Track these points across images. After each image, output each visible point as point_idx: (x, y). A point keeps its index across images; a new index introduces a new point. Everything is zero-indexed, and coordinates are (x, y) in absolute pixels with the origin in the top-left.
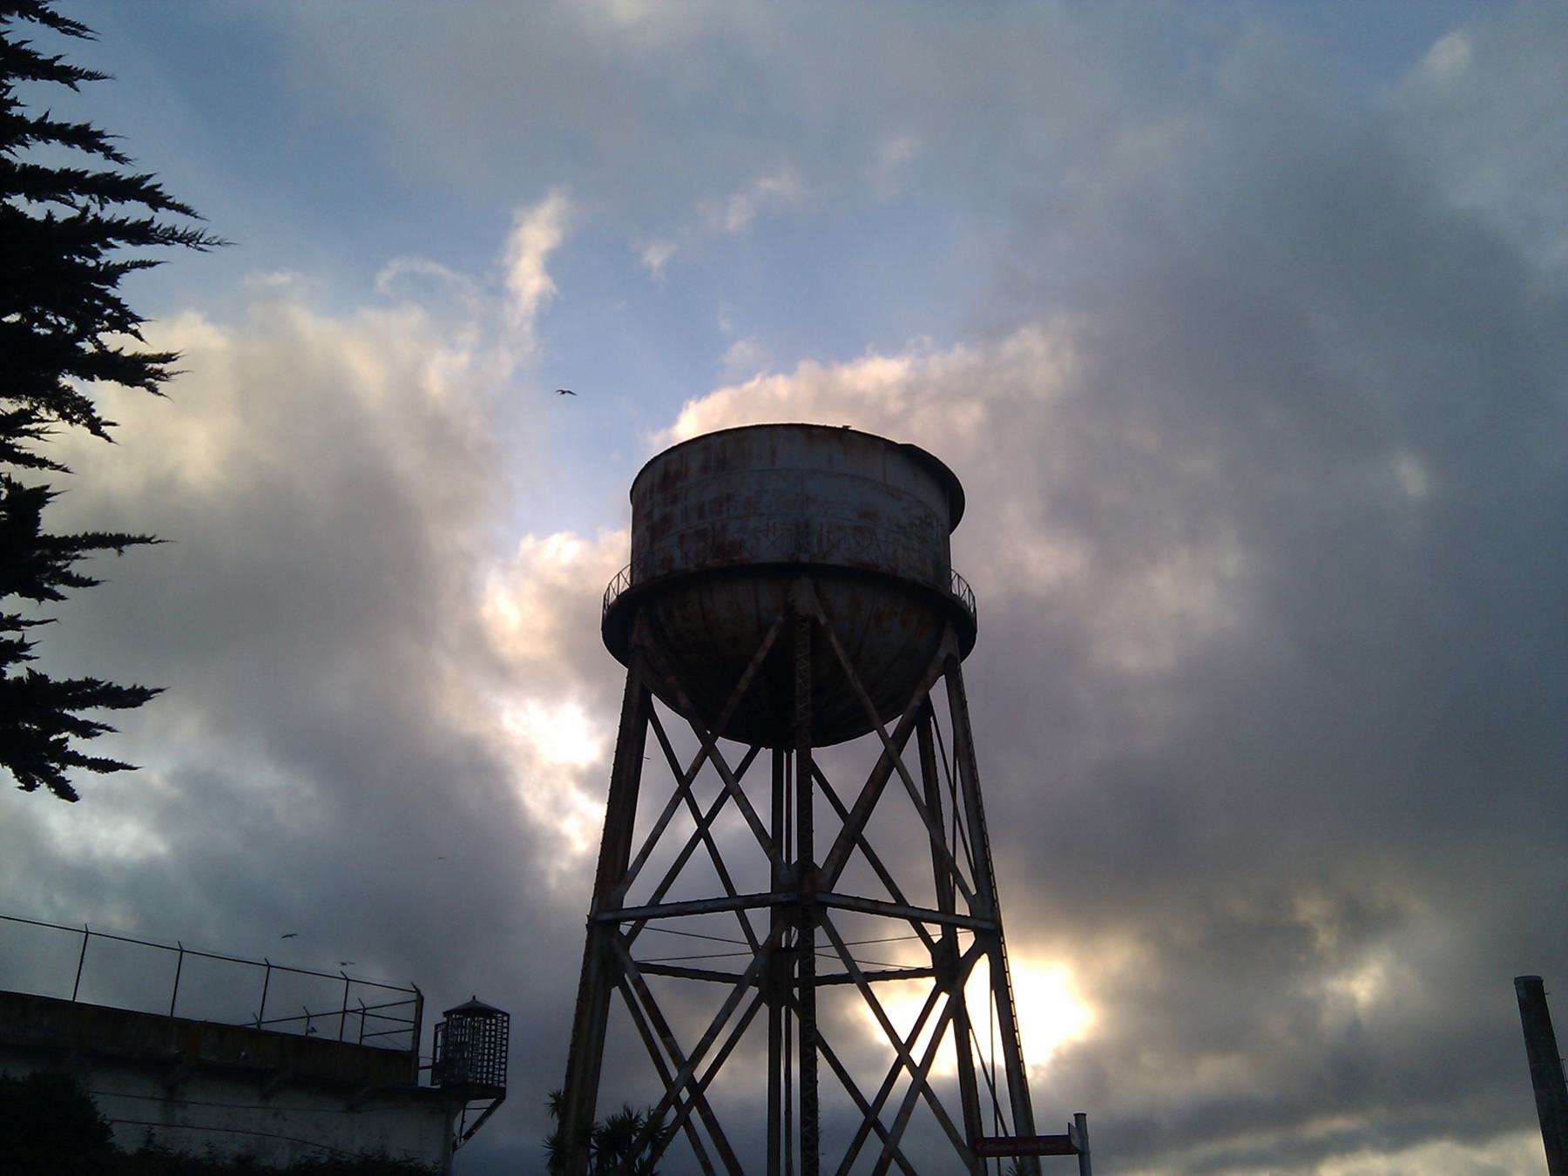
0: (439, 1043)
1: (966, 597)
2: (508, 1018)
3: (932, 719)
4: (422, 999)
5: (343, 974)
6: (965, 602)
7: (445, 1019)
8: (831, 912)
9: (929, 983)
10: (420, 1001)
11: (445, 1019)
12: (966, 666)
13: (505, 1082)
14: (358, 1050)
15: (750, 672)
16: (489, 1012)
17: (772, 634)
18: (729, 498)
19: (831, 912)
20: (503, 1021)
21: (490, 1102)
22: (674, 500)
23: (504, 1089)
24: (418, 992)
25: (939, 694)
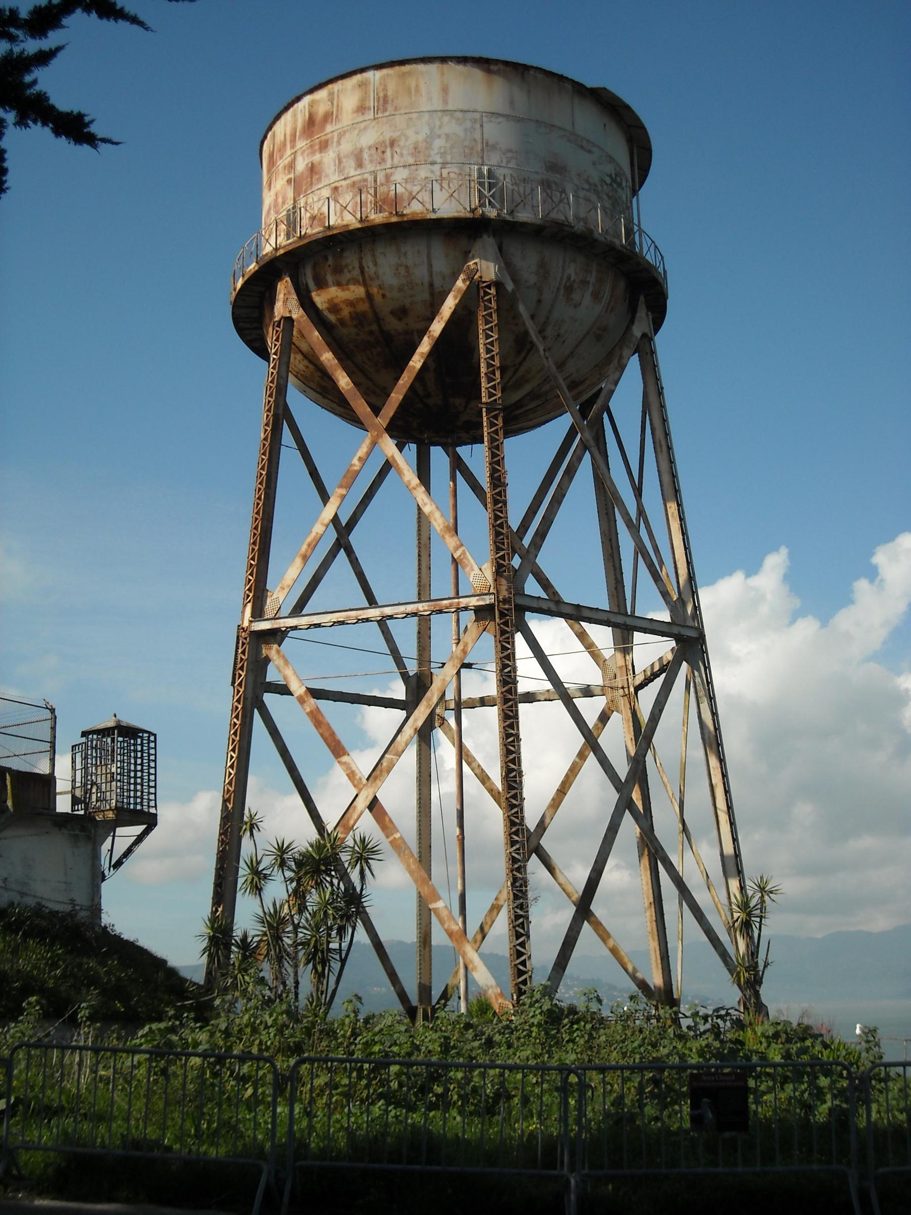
0: (78, 766)
1: (661, 270)
2: (155, 738)
4: (56, 717)
7: (84, 740)
13: (156, 807)
15: (425, 346)
16: (129, 732)
17: (450, 304)
18: (392, 143)
21: (139, 829)
22: (324, 146)
23: (156, 815)
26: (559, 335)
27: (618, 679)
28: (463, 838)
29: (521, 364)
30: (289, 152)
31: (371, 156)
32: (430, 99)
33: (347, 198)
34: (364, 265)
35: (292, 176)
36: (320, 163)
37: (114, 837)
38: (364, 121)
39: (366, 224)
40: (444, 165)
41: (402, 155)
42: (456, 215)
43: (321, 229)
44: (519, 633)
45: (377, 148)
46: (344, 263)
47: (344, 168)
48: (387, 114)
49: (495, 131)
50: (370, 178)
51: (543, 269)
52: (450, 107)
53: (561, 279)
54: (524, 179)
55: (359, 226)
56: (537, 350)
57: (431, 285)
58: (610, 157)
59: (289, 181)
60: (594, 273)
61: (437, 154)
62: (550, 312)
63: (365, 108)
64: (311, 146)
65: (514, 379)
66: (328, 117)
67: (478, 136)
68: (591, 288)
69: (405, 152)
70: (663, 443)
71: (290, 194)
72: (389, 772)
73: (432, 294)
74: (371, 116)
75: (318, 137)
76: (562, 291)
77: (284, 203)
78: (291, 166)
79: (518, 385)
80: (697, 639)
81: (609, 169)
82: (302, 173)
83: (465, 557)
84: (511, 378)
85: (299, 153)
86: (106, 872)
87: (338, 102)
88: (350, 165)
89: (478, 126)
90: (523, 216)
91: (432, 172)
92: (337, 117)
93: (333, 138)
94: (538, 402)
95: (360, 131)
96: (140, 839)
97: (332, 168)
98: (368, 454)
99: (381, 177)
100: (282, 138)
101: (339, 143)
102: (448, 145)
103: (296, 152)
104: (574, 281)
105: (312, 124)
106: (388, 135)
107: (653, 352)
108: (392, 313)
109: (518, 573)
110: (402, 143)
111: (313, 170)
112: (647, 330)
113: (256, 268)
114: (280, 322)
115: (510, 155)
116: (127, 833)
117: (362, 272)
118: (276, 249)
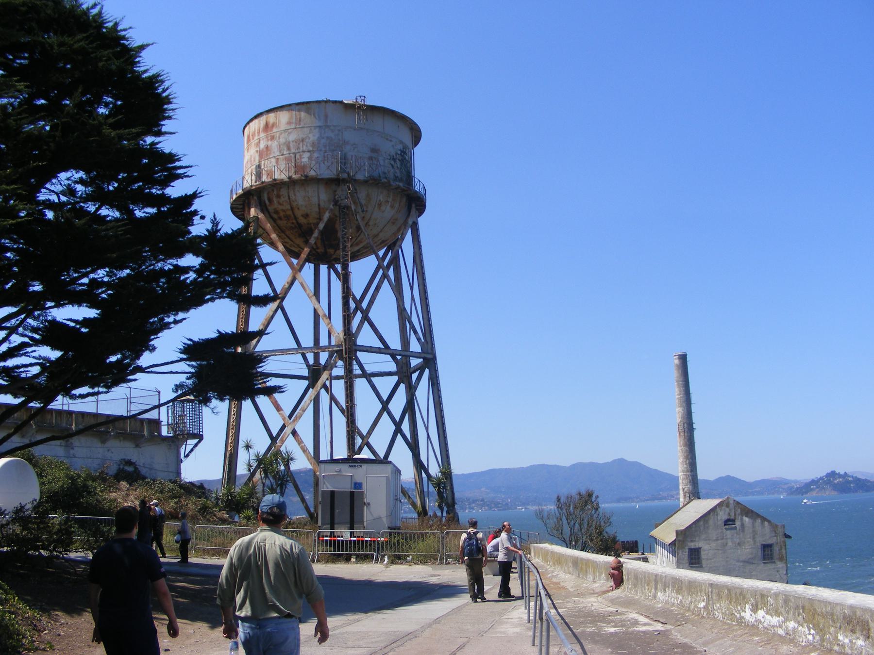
1: (423, 192)
9: (395, 379)
13: (202, 432)
18: (303, 140)
19: (359, 354)
21: (196, 441)
23: (203, 435)
26: (375, 224)
27: (404, 368)
28: (332, 441)
29: (359, 236)
30: (256, 137)
33: (283, 165)
34: (290, 195)
35: (258, 149)
36: (271, 146)
37: (186, 445)
38: (291, 129)
41: (307, 146)
42: (330, 177)
43: (271, 180)
45: (296, 142)
52: (329, 124)
53: (377, 201)
55: (288, 180)
60: (391, 197)
62: (372, 215)
63: (291, 123)
68: (390, 204)
69: (308, 145)
71: (257, 158)
72: (300, 418)
73: (319, 209)
74: (294, 127)
76: (377, 206)
77: (254, 161)
78: (258, 144)
79: (357, 244)
80: (433, 359)
81: (400, 147)
82: (263, 149)
86: (183, 459)
94: (367, 250)
95: (289, 133)
96: (196, 445)
97: (276, 149)
99: (298, 156)
100: (254, 130)
106: (301, 136)
110: (307, 140)
113: (242, 193)
115: (354, 146)
116: (191, 442)
117: (289, 198)
118: (251, 186)
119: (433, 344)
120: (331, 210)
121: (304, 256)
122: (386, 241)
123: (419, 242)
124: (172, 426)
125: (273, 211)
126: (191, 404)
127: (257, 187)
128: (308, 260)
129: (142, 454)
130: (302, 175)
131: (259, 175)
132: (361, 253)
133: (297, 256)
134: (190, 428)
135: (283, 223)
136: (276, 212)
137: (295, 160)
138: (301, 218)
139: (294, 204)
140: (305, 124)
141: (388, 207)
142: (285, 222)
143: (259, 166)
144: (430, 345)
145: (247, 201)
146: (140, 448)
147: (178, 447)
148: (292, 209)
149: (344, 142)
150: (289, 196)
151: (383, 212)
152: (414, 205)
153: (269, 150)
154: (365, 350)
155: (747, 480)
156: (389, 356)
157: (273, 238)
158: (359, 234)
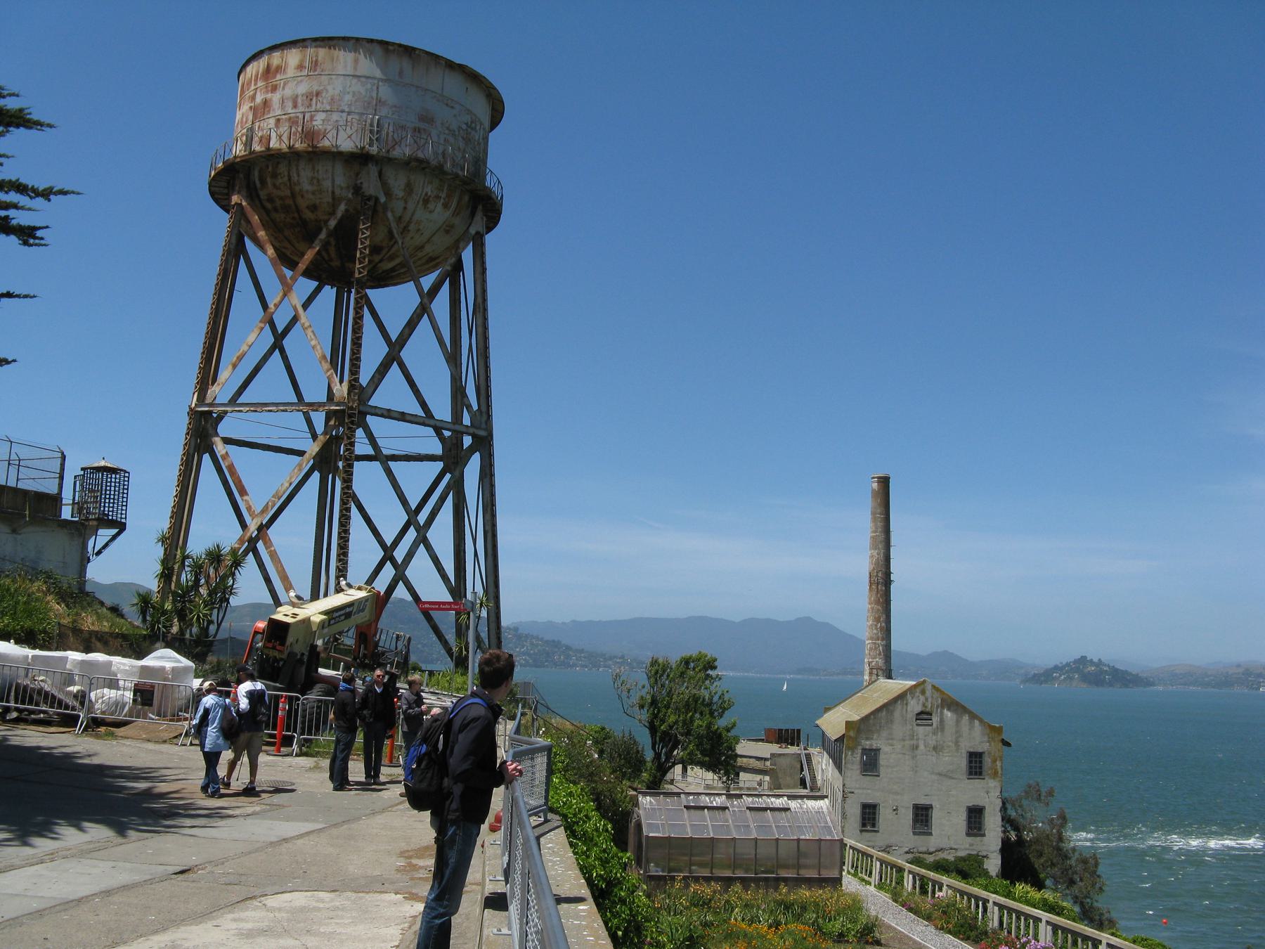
0: (77, 489)
3: (461, 273)
4: (65, 457)
5: (7, 437)
6: (494, 192)
7: (82, 473)
8: (369, 418)
9: (439, 466)
10: (64, 457)
11: (82, 473)
12: (489, 239)
14: (16, 491)
18: (317, 94)
19: (370, 420)
20: (124, 477)
21: (115, 531)
22: (274, 89)
23: (125, 524)
24: (63, 453)
25: (467, 255)
26: (419, 230)
29: (392, 246)
30: (253, 87)
31: (302, 101)
32: (346, 66)
33: (284, 129)
34: (291, 175)
36: (271, 100)
38: (301, 76)
39: (292, 150)
40: (349, 113)
41: (323, 103)
44: (361, 429)
46: (278, 172)
47: (285, 107)
48: (316, 73)
49: (385, 92)
50: (301, 116)
51: (409, 188)
52: (358, 73)
53: (421, 194)
54: (402, 127)
55: (287, 150)
56: (398, 243)
57: (333, 193)
58: (469, 110)
59: (251, 108)
60: (445, 191)
61: (346, 105)
62: (413, 215)
63: (302, 67)
64: (266, 87)
65: (388, 255)
66: (279, 69)
67: (374, 95)
69: (325, 101)
70: (481, 306)
71: (251, 117)
73: (334, 199)
75: (273, 81)
76: (421, 202)
77: (246, 122)
78: (253, 98)
79: (392, 258)
80: (487, 437)
81: (467, 118)
82: (259, 104)
83: (332, 377)
84: (386, 254)
85: (258, 90)
87: (286, 59)
88: (289, 104)
89: (375, 88)
90: (397, 153)
91: (341, 117)
92: (284, 70)
93: (280, 83)
95: (298, 83)
96: (114, 537)
98: (280, 302)
99: (307, 116)
101: (284, 88)
102: (354, 99)
103: (257, 89)
104: (430, 196)
105: (268, 72)
106: (316, 88)
107: (483, 245)
108: (308, 207)
109: (365, 390)
110: (324, 95)
111: (266, 103)
112: (480, 230)
114: (234, 206)
115: (394, 109)
116: (105, 534)
117: (290, 180)
118: (235, 157)
119: (489, 416)
120: (349, 201)
121: (302, 266)
122: (438, 258)
123: (483, 263)
124: (79, 507)
125: (265, 197)
126: (114, 476)
127: (243, 159)
128: (308, 274)
129: (21, 544)
130: (309, 145)
131: (249, 143)
132: (396, 273)
133: (292, 265)
134: (109, 511)
135: (280, 217)
136: (270, 200)
137: (304, 123)
138: (307, 211)
139: (297, 188)
140: (322, 71)
141: (440, 205)
142: (283, 216)
143: (251, 130)
144: (485, 418)
145: (231, 182)
146: (20, 534)
147: (84, 538)
148: (293, 196)
149: (380, 101)
150: (289, 177)
151: (431, 212)
152: (480, 207)
153: (268, 107)
154: (379, 413)
155: (595, 620)
156: (431, 429)
157: (260, 238)
158: (392, 243)
